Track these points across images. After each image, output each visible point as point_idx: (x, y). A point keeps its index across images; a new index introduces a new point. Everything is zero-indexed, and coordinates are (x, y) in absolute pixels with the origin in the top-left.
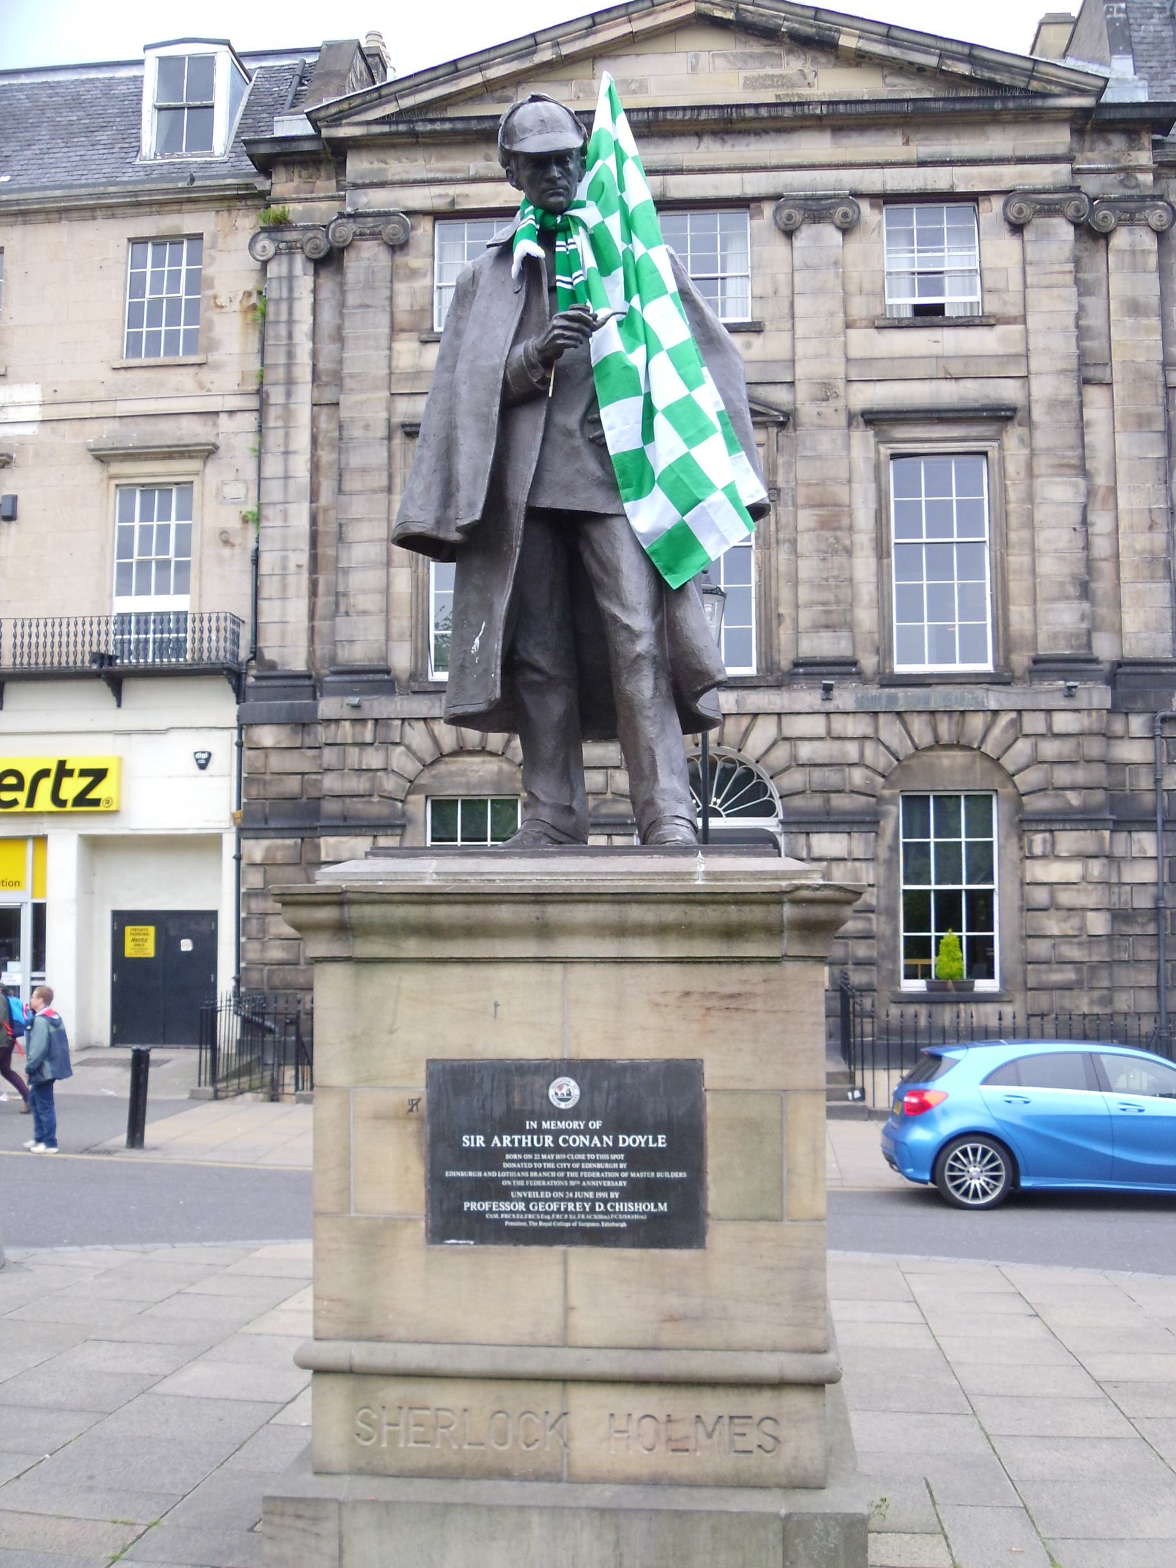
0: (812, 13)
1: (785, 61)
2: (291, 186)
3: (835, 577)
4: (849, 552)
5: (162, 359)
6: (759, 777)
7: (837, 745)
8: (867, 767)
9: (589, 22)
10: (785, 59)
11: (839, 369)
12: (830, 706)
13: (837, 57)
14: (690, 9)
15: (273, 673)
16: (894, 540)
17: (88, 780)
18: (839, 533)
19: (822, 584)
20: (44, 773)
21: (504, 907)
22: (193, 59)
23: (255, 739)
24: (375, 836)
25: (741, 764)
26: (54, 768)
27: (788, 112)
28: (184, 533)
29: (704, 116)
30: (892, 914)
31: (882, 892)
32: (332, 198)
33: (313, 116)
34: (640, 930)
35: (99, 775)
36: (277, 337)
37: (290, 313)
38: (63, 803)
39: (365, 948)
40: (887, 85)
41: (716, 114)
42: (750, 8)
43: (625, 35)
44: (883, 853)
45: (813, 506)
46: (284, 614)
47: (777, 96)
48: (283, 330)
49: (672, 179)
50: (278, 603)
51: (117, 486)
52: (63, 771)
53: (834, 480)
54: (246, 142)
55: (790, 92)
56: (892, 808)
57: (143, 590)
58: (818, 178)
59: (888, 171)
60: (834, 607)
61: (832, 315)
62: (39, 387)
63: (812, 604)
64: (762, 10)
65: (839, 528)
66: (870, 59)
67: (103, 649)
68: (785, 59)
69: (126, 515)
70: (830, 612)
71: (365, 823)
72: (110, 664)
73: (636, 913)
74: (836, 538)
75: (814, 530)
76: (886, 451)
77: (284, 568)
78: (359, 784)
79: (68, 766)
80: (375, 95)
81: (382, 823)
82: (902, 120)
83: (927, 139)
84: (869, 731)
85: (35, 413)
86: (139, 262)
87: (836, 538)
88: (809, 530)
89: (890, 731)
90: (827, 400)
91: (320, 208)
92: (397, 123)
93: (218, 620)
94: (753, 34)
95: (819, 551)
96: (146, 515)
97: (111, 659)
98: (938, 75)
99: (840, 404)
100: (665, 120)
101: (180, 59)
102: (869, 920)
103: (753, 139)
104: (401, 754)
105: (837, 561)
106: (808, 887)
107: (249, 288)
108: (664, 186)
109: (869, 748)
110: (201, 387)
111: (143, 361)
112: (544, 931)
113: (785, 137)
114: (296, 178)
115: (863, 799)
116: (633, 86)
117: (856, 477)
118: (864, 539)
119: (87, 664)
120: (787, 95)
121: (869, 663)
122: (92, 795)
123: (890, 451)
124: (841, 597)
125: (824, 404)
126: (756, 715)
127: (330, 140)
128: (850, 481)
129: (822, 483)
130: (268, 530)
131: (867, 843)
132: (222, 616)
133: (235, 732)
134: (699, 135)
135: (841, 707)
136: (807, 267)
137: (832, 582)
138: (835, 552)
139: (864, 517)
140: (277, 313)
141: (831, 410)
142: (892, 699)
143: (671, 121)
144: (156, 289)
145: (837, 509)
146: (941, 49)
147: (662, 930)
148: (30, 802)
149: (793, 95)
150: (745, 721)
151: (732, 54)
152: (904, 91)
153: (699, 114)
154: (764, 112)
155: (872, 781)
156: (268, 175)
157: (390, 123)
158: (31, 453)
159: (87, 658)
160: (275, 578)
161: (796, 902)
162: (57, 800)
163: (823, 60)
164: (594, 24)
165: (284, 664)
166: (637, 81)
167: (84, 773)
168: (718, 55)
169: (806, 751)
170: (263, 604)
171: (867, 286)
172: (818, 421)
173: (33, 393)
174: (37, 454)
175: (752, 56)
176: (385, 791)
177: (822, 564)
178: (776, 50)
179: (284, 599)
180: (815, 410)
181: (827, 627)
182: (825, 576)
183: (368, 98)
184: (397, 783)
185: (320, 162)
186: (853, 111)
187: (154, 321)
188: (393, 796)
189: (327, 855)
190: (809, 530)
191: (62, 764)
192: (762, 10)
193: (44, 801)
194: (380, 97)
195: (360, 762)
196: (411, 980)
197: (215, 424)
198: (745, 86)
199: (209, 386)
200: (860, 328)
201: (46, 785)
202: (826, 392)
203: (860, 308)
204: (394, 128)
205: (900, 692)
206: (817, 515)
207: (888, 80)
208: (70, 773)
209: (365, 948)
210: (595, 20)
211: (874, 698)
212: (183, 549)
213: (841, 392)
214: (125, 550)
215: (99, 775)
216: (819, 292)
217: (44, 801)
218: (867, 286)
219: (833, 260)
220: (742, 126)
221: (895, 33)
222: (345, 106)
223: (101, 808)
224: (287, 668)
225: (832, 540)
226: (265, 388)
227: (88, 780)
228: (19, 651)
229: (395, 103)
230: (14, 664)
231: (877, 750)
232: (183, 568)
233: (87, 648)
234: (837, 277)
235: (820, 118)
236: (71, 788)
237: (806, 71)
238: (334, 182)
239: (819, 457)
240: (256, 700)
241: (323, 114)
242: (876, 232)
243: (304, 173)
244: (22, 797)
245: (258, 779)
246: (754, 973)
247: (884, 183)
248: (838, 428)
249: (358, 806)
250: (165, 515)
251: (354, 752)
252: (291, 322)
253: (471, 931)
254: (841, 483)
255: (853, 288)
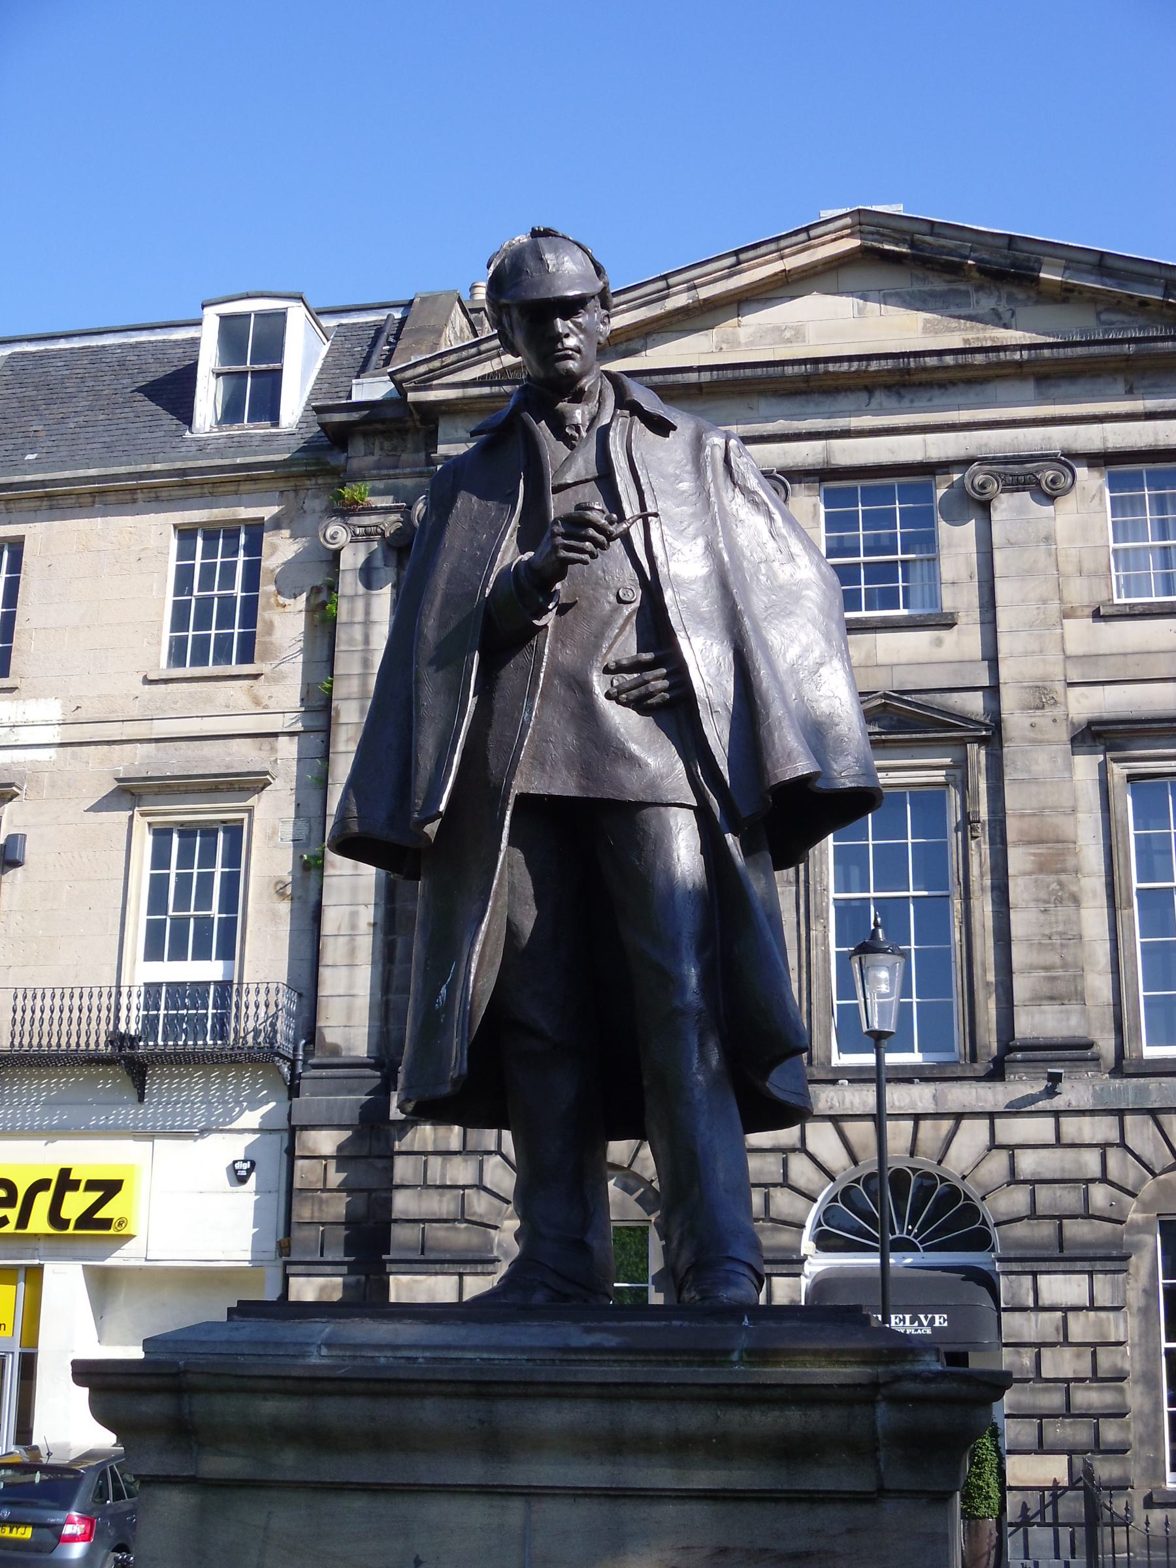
0: (1005, 241)
1: (973, 299)
2: (370, 460)
3: (1060, 934)
4: (1076, 900)
5: (211, 669)
6: (967, 1197)
7: (1070, 1153)
8: (1112, 1184)
9: (732, 260)
10: (974, 298)
11: (1057, 671)
12: (1058, 1103)
13: (1039, 293)
14: (855, 243)
15: (336, 1060)
16: (1136, 885)
17: (96, 1195)
18: (1063, 877)
19: (1043, 943)
20: (42, 1185)
21: (429, 1403)
22: (261, 316)
23: (310, 1144)
24: (461, 1275)
25: (943, 1180)
26: (54, 1176)
27: (979, 359)
28: (231, 884)
29: (874, 366)
30: (1151, 1382)
31: (1137, 1351)
32: (420, 475)
33: (398, 377)
34: (646, 1445)
35: (110, 1188)
36: (351, 641)
37: (367, 613)
38: (65, 1224)
39: (216, 1465)
40: (1104, 323)
41: (890, 364)
42: (928, 239)
43: (776, 274)
44: (1135, 1298)
45: (1029, 843)
46: (351, 985)
47: (966, 341)
48: (358, 633)
49: (836, 443)
50: (344, 972)
51: (150, 824)
52: (66, 1182)
53: (1054, 808)
54: (315, 409)
55: (981, 335)
56: (1148, 1238)
57: (178, 954)
58: (1021, 437)
59: (1108, 426)
60: (1060, 973)
61: (1045, 602)
62: (58, 703)
63: (1032, 968)
64: (943, 242)
65: (1064, 871)
66: (1080, 293)
67: (122, 1028)
68: (974, 298)
69: (160, 859)
70: (1053, 979)
71: (448, 1257)
72: (132, 1047)
73: (637, 1417)
74: (1060, 883)
75: (1030, 873)
76: (1118, 772)
77: (353, 926)
78: (443, 1205)
79: (72, 1177)
80: (473, 351)
81: (470, 1256)
82: (1123, 365)
83: (1155, 385)
84: (1114, 1136)
85: (53, 735)
86: (186, 552)
87: (1060, 883)
88: (1025, 874)
89: (1141, 1134)
90: (1043, 708)
91: (405, 486)
92: (499, 383)
93: (268, 991)
94: (933, 269)
95: (1037, 900)
96: (185, 860)
97: (133, 1040)
98: (1165, 310)
99: (1058, 712)
100: (827, 373)
101: (247, 316)
102: (1121, 1391)
103: (937, 392)
104: (496, 1166)
105: (1062, 912)
106: (915, 1377)
107: (319, 583)
108: (827, 450)
109: (1114, 1156)
110: (257, 702)
111: (188, 671)
112: (495, 1444)
113: (978, 388)
114: (377, 451)
115: (1108, 1226)
116: (787, 334)
117: (1083, 805)
118: (1093, 884)
119: (102, 1046)
120: (978, 339)
121: (1106, 1045)
122: (101, 1214)
123: (1127, 771)
124: (1070, 959)
125: (1038, 713)
126: (959, 1117)
127: (418, 405)
128: (1074, 810)
129: (1039, 814)
130: (334, 879)
131: (1114, 1285)
132: (273, 987)
133: (286, 1136)
134: (869, 390)
135: (1074, 1103)
136: (1010, 544)
137: (1057, 941)
138: (1060, 901)
139: (1092, 856)
140: (352, 612)
141: (1049, 721)
142: (1142, 1092)
143: (834, 373)
144: (206, 584)
145: (1060, 845)
146: (1167, 280)
147: (680, 1447)
148: (23, 1221)
149: (985, 339)
150: (947, 1125)
151: (908, 293)
152: (1125, 329)
153: (868, 365)
154: (949, 360)
155: (1119, 1201)
156: (344, 448)
157: (491, 384)
158: (46, 780)
159: (103, 1038)
160: (341, 940)
161: (897, 1401)
162: (55, 1217)
163: (1021, 296)
164: (739, 263)
165: (349, 1049)
166: (791, 328)
167: (92, 1185)
168: (891, 295)
169: (1028, 1163)
170: (326, 974)
171: (1088, 565)
172: (1032, 735)
173: (52, 709)
174: (53, 785)
175: (933, 295)
176: (474, 1214)
177: (1042, 917)
178: (962, 287)
179: (351, 965)
180: (1027, 722)
181: (1052, 998)
182: (1047, 932)
183: (464, 354)
184: (491, 1204)
185: (407, 431)
186: (1062, 356)
187: (203, 622)
188: (486, 1221)
189: (397, 1296)
190: (1025, 874)
191: (65, 1173)
192: (943, 242)
193: (39, 1222)
194: (480, 353)
195: (443, 1176)
196: (286, 1517)
197: (273, 750)
198: (925, 330)
199: (265, 702)
200: (1081, 617)
201: (43, 1201)
202: (1041, 697)
203: (1079, 592)
204: (496, 389)
205: (1152, 1083)
206: (1034, 854)
207: (1104, 317)
208: (75, 1185)
209: (216, 1465)
210: (739, 257)
211: (1118, 1091)
212: (230, 901)
213: (1060, 699)
214: (157, 901)
215: (110, 1188)
216: (1027, 574)
217: (39, 1222)
218: (1088, 565)
219: (1043, 534)
220: (924, 377)
221: (1109, 262)
222: (436, 364)
223: (111, 1232)
224: (352, 1054)
225: (1054, 886)
226: (334, 704)
227: (96, 1195)
228: (18, 1028)
229: (497, 360)
230: (12, 1044)
231: (1124, 1160)
232: (229, 928)
233: (103, 1026)
234: (1050, 555)
235: (1019, 364)
236: (75, 1204)
237: (1001, 309)
238: (422, 455)
239: (1034, 780)
240: (312, 1095)
241: (409, 374)
242: (1097, 500)
243: (387, 445)
244: (13, 1214)
245: (313, 1197)
246: (829, 1517)
247: (1105, 439)
248: (1057, 743)
249: (438, 1233)
250: (208, 859)
251: (435, 1162)
252: (368, 623)
253: (379, 1441)
254: (1064, 813)
255: (1068, 568)
